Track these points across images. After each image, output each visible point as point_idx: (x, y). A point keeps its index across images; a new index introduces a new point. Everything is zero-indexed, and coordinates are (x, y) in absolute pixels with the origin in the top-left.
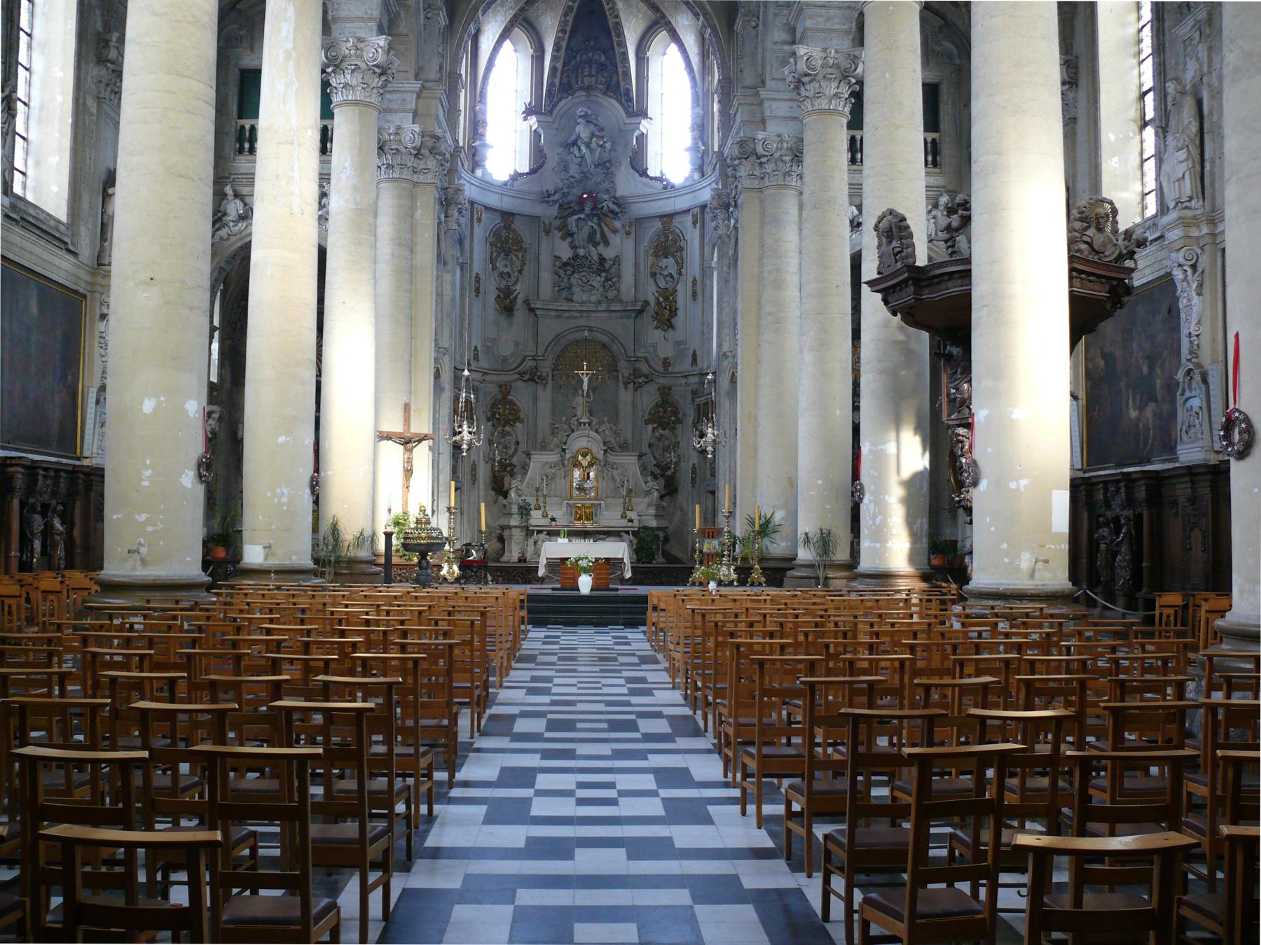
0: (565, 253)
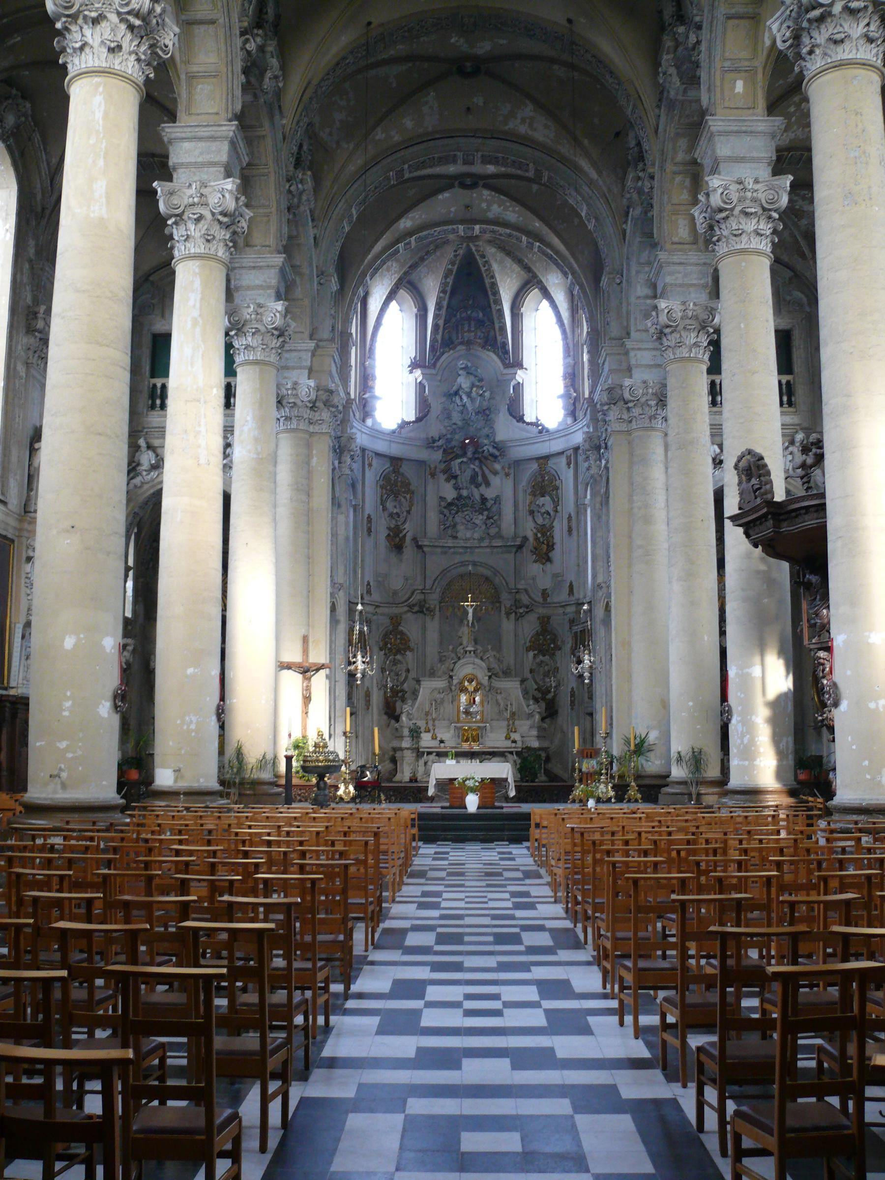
0: (450, 494)
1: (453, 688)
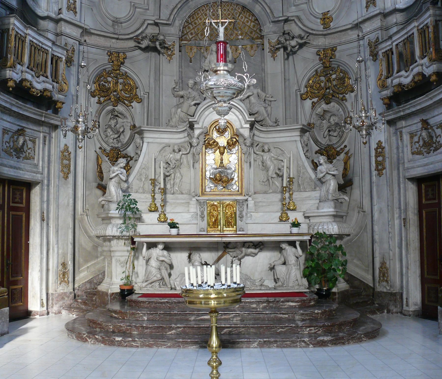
1: (195, 141)
